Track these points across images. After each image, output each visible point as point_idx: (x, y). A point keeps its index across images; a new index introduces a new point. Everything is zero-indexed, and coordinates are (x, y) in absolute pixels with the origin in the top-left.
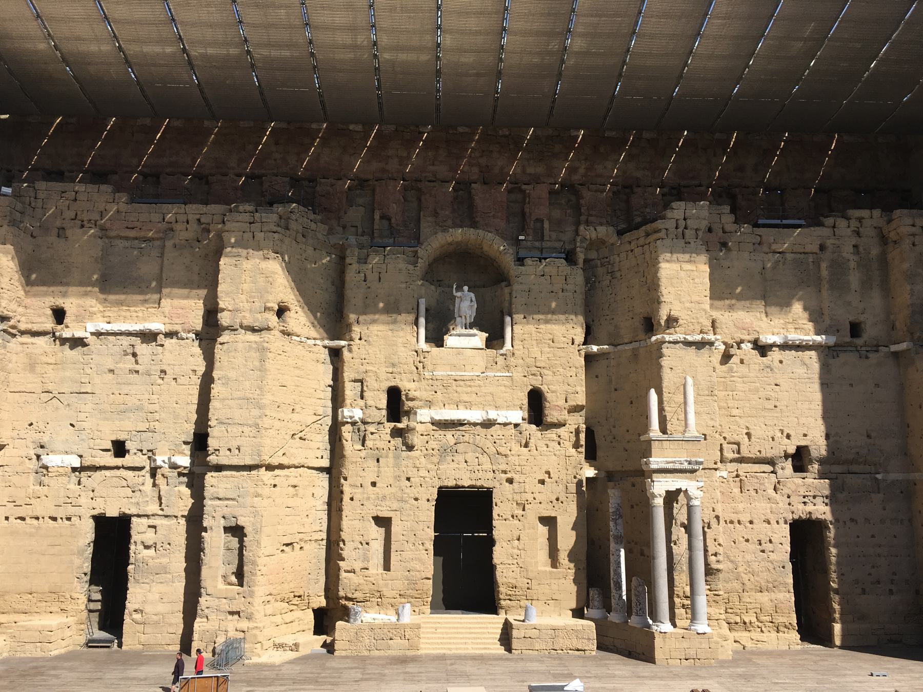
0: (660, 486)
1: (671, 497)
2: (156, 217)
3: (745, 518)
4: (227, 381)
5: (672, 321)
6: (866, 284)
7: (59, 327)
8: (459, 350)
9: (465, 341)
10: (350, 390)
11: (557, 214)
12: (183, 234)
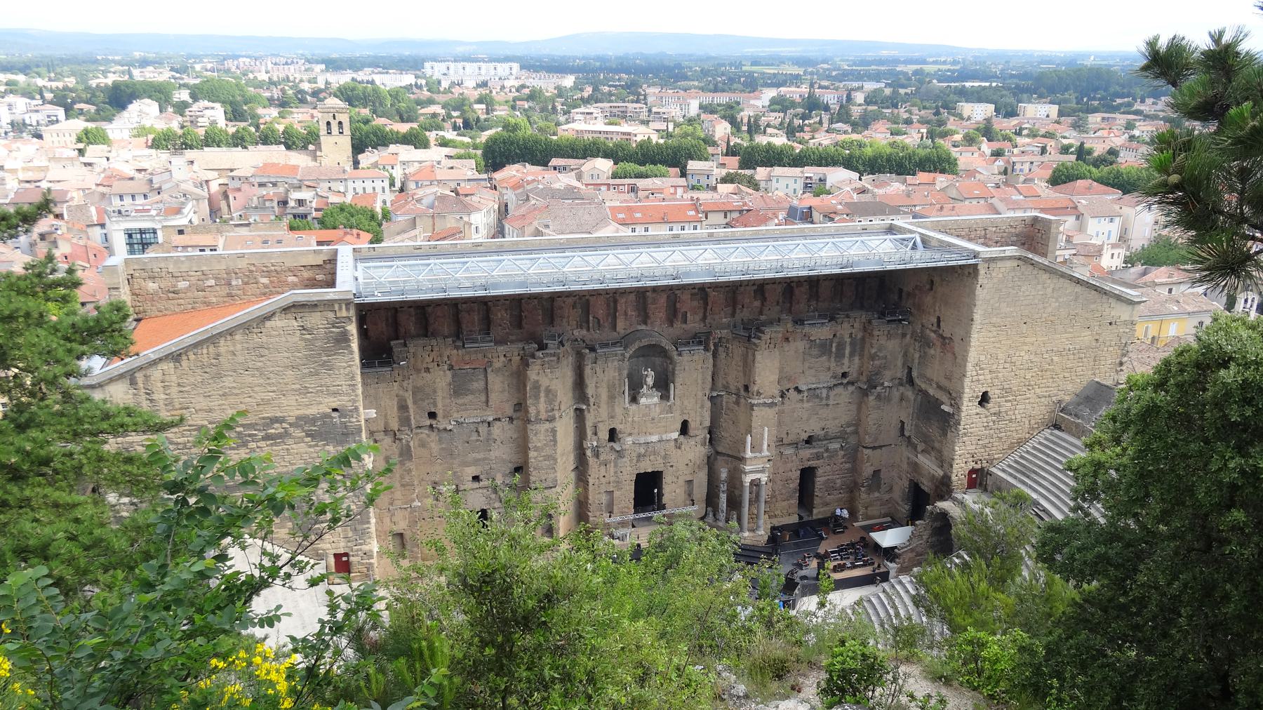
0: (747, 480)
1: (752, 482)
2: (480, 356)
3: (781, 471)
4: (536, 449)
5: (759, 394)
6: (852, 354)
7: (434, 422)
8: (647, 406)
9: (650, 399)
10: (589, 432)
11: (695, 303)
12: (498, 364)
